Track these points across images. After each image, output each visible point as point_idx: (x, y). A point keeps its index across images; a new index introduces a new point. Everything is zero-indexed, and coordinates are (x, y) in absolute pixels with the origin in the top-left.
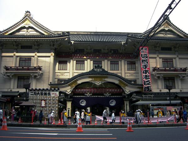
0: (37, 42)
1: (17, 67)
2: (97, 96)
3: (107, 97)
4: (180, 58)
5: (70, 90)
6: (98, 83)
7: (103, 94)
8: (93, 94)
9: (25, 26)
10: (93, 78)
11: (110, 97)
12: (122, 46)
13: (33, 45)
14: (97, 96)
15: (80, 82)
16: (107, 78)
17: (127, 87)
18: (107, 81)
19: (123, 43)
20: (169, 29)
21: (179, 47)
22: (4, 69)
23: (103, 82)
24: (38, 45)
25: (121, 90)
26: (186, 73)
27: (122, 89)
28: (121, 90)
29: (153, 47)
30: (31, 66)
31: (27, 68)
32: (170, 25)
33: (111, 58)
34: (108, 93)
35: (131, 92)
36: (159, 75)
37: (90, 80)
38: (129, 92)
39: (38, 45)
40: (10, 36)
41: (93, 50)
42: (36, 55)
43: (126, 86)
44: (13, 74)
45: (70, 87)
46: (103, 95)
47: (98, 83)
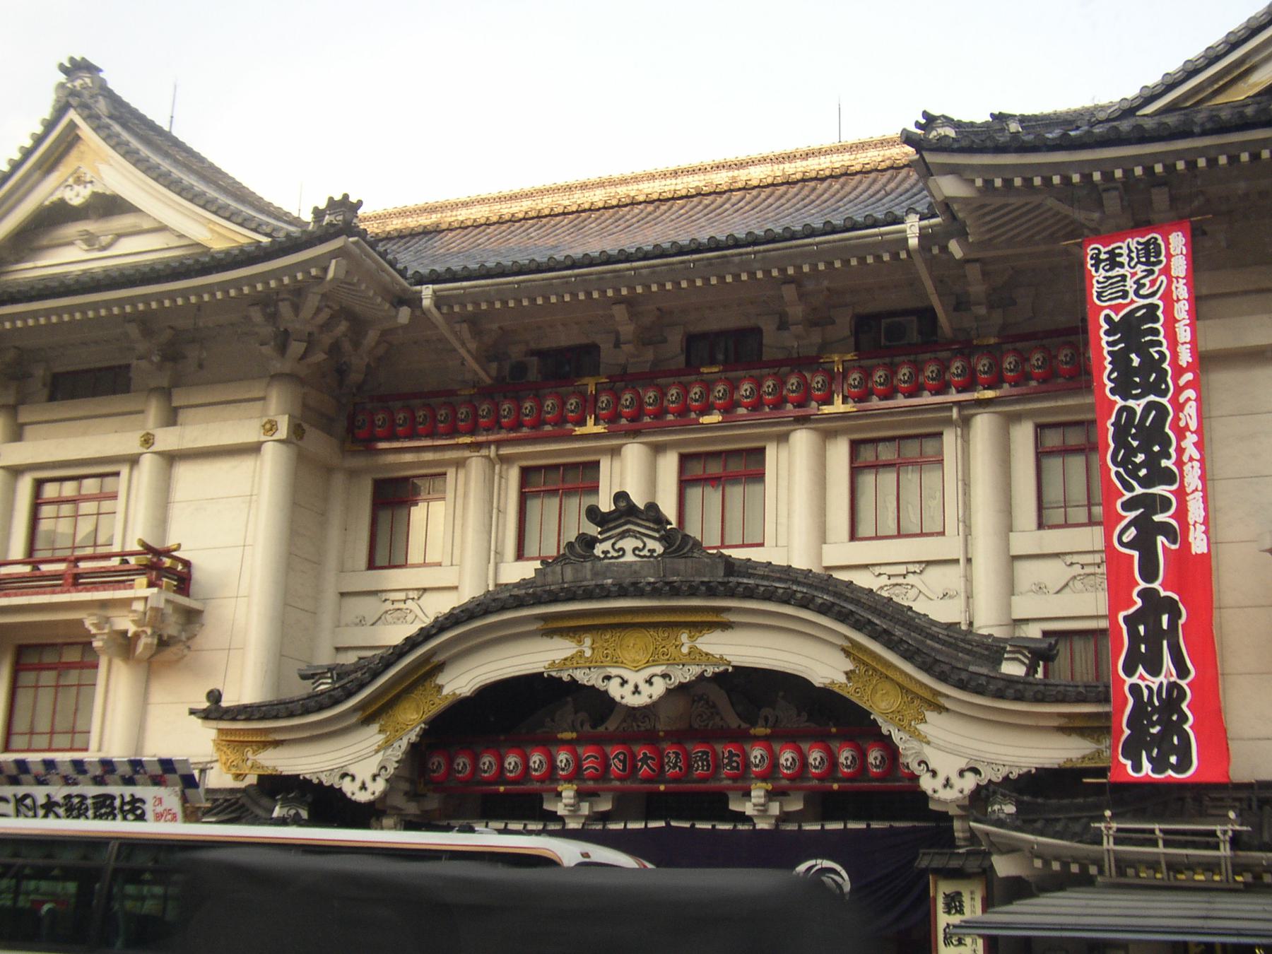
0: (146, 322)
5: (372, 765)
6: (636, 691)
7: (725, 801)
9: (62, 203)
15: (462, 681)
16: (726, 626)
17: (935, 726)
19: (912, 228)
25: (874, 756)
28: (874, 756)
31: (61, 567)
33: (849, 407)
34: (758, 794)
35: (989, 774)
37: (568, 653)
38: (970, 782)
39: (172, 354)
41: (675, 340)
42: (148, 440)
43: (931, 716)
45: (375, 727)
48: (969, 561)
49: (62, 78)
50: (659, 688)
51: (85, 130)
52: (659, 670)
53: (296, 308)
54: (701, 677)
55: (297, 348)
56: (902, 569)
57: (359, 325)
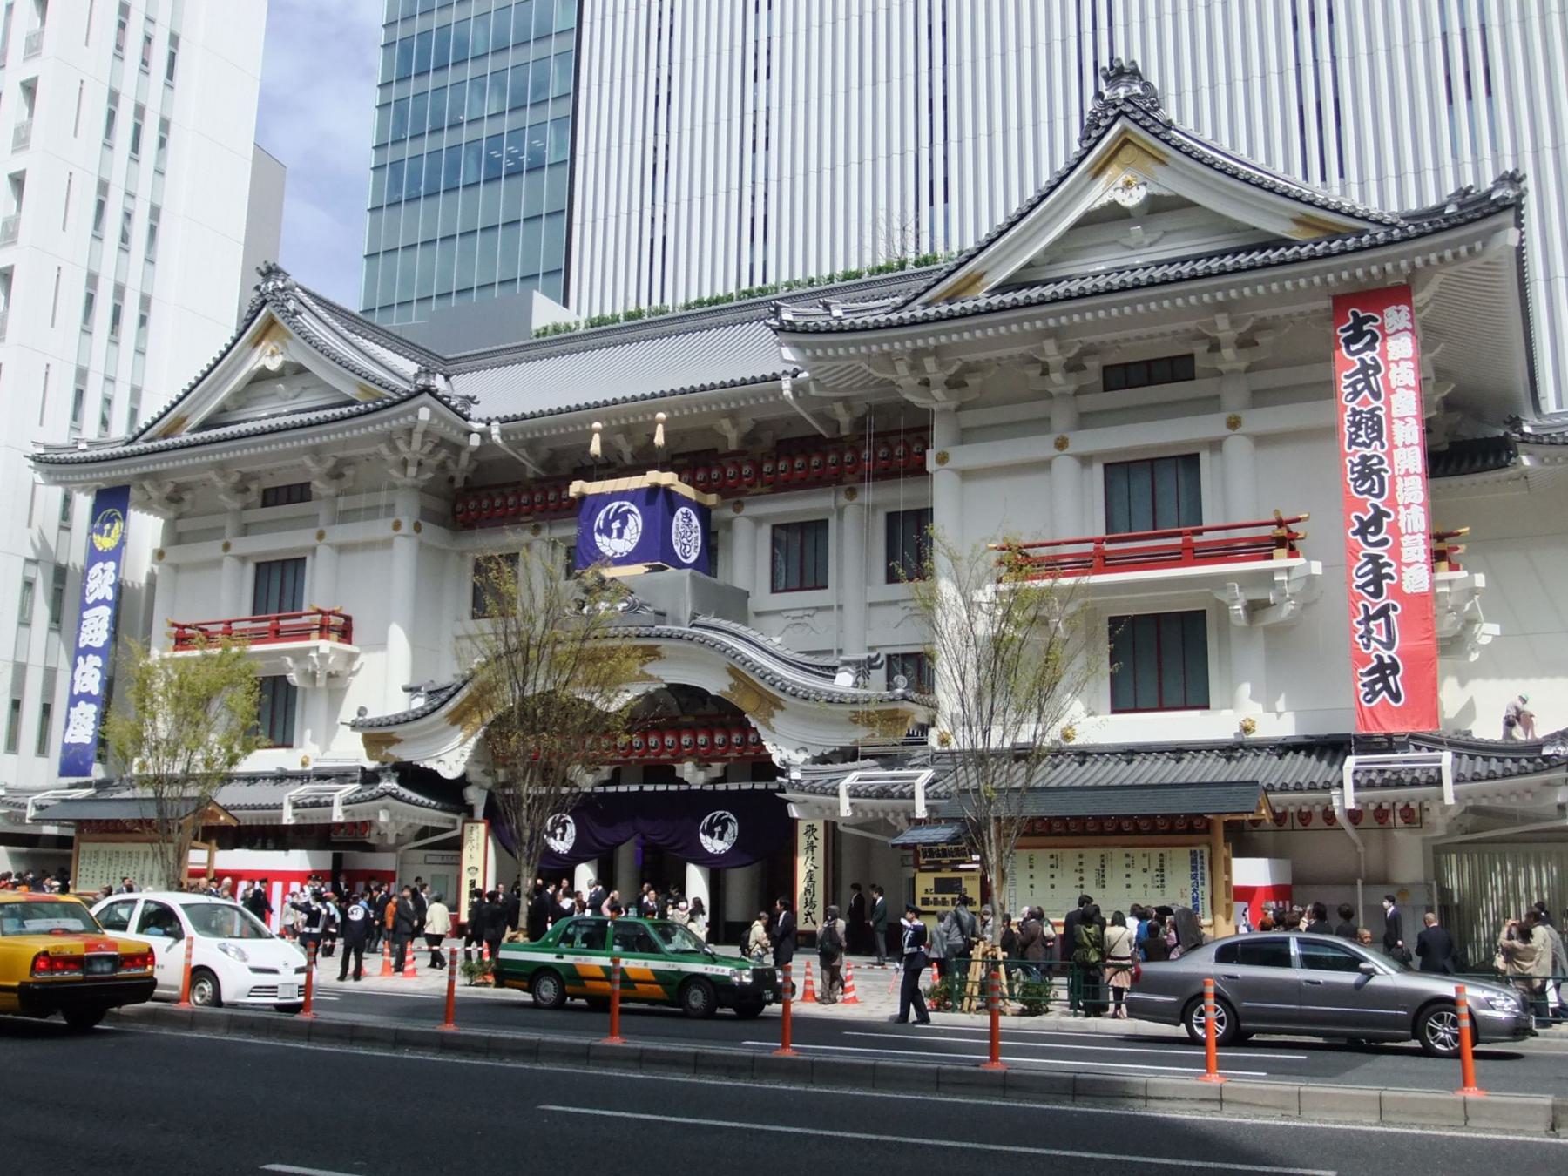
1: (229, 623)
3: (691, 793)
4: (1261, 441)
11: (715, 791)
20: (1156, 190)
26: (1272, 572)
27: (755, 729)
48: (840, 607)
49: (259, 280)
51: (278, 317)
53: (409, 444)
54: (658, 690)
55: (412, 470)
56: (800, 613)
57: (457, 449)
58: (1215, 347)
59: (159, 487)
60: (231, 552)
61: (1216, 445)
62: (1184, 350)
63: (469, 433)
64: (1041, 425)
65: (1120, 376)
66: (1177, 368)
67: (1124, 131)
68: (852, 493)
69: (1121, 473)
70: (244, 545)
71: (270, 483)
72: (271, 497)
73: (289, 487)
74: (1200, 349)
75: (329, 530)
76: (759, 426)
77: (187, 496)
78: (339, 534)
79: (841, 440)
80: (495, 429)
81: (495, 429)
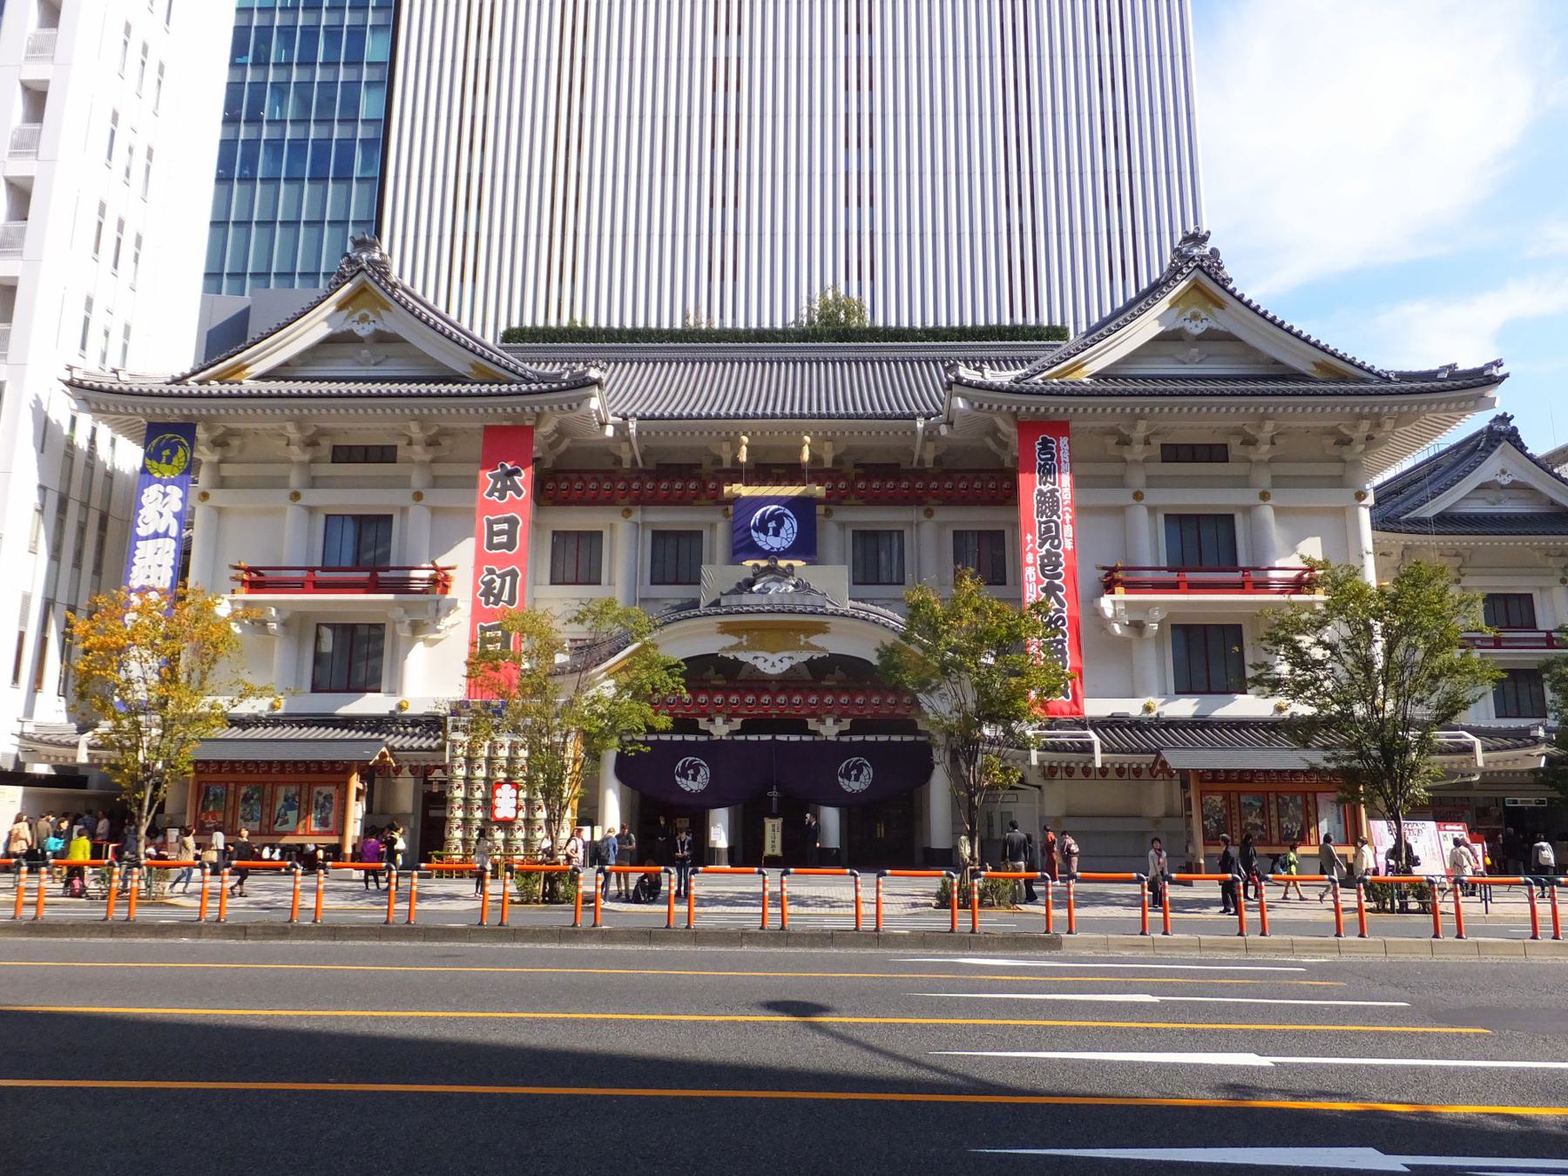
1: (312, 570)
2: (769, 737)
8: (745, 730)
9: (351, 332)
10: (747, 631)
12: (920, 438)
13: (401, 443)
14: (769, 737)
18: (823, 649)
20: (1214, 325)
21: (1279, 441)
22: (234, 579)
23: (803, 657)
24: (432, 443)
29: (1111, 441)
30: (393, 563)
32: (1220, 305)
36: (1137, 617)
40: (264, 387)
44: (286, 615)
46: (801, 728)
47: (772, 663)
50: (786, 665)
52: (787, 654)
58: (1250, 442)
59: (208, 429)
60: (301, 502)
61: (1248, 510)
62: (1218, 440)
63: (603, 424)
64: (1119, 482)
65: (1173, 453)
66: (1216, 453)
67: (1195, 279)
68: (929, 513)
69: (1182, 524)
70: (312, 497)
71: (342, 441)
72: (343, 454)
73: (366, 448)
74: (1234, 444)
75: (427, 493)
76: (849, 451)
77: (235, 442)
78: (436, 497)
79: (926, 470)
80: (633, 426)
81: (633, 426)
